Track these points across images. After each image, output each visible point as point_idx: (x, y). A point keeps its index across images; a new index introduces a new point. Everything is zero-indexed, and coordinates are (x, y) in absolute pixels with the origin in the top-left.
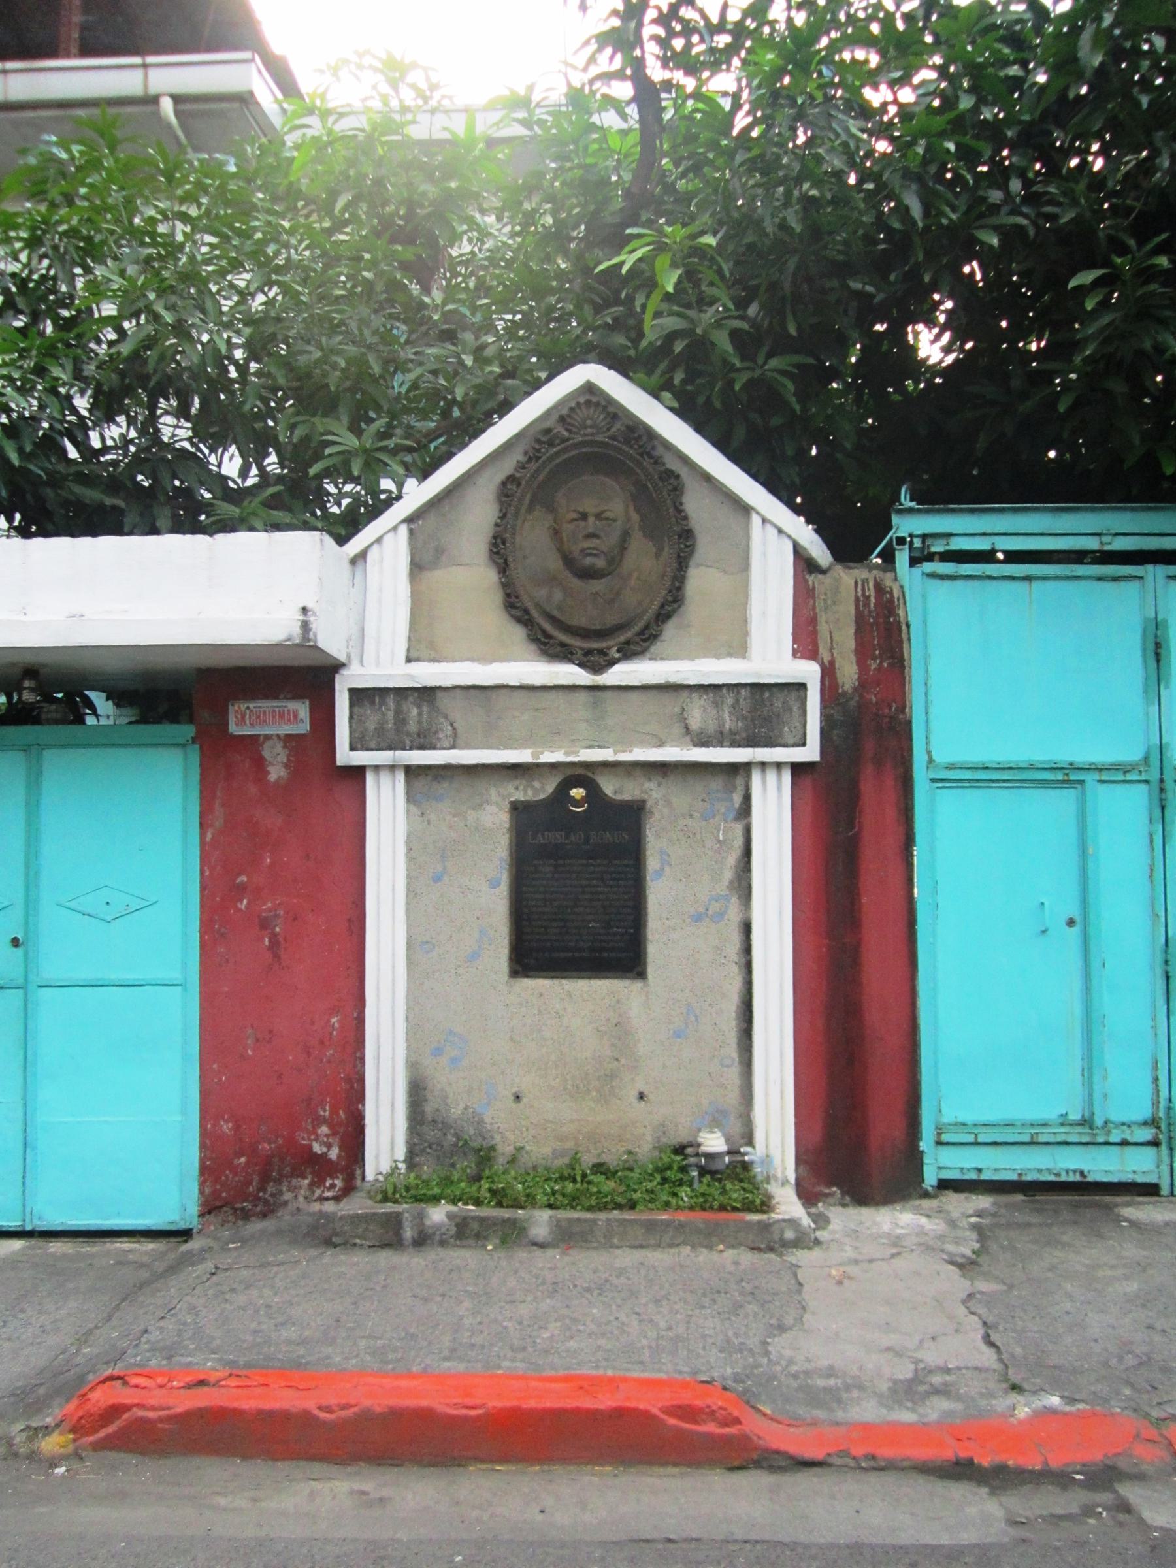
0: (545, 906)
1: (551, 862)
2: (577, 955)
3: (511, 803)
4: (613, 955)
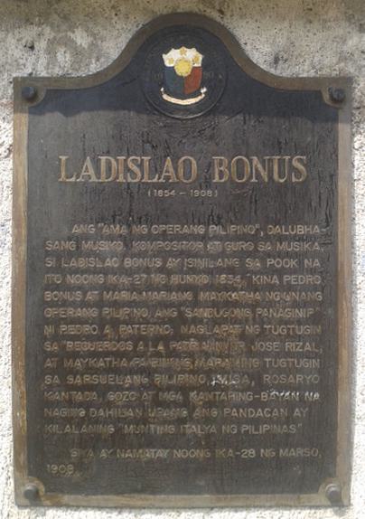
0: (102, 337)
1: (118, 229)
2: (179, 454)
3: (17, 82)
4: (267, 453)
